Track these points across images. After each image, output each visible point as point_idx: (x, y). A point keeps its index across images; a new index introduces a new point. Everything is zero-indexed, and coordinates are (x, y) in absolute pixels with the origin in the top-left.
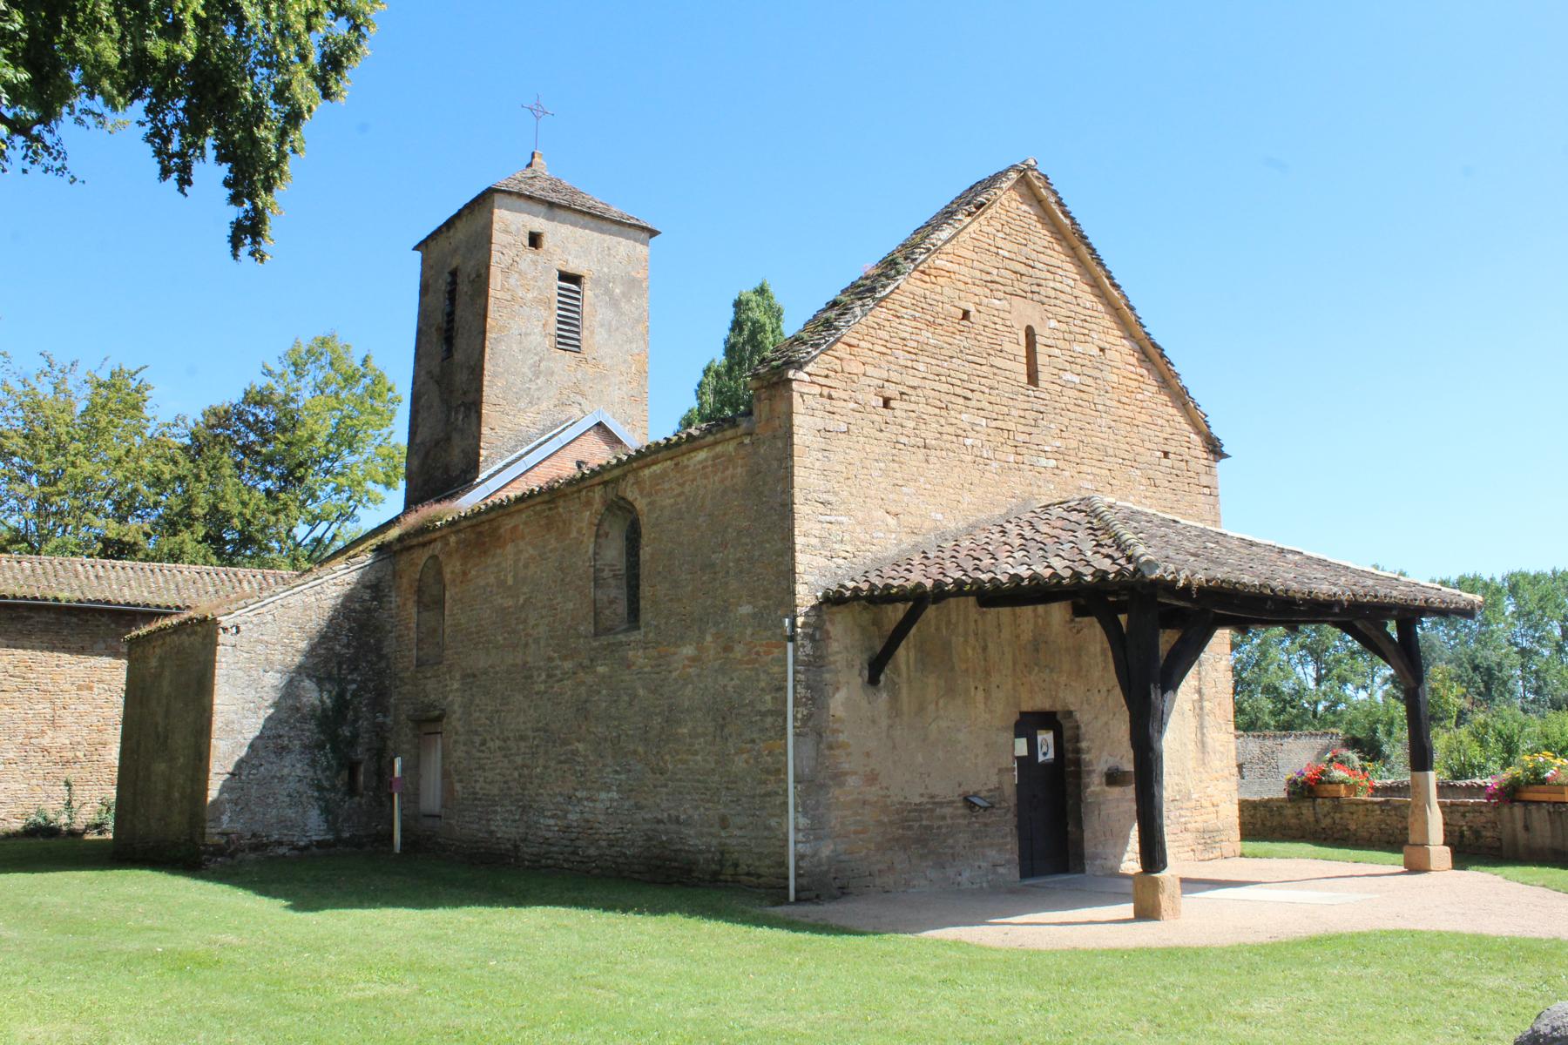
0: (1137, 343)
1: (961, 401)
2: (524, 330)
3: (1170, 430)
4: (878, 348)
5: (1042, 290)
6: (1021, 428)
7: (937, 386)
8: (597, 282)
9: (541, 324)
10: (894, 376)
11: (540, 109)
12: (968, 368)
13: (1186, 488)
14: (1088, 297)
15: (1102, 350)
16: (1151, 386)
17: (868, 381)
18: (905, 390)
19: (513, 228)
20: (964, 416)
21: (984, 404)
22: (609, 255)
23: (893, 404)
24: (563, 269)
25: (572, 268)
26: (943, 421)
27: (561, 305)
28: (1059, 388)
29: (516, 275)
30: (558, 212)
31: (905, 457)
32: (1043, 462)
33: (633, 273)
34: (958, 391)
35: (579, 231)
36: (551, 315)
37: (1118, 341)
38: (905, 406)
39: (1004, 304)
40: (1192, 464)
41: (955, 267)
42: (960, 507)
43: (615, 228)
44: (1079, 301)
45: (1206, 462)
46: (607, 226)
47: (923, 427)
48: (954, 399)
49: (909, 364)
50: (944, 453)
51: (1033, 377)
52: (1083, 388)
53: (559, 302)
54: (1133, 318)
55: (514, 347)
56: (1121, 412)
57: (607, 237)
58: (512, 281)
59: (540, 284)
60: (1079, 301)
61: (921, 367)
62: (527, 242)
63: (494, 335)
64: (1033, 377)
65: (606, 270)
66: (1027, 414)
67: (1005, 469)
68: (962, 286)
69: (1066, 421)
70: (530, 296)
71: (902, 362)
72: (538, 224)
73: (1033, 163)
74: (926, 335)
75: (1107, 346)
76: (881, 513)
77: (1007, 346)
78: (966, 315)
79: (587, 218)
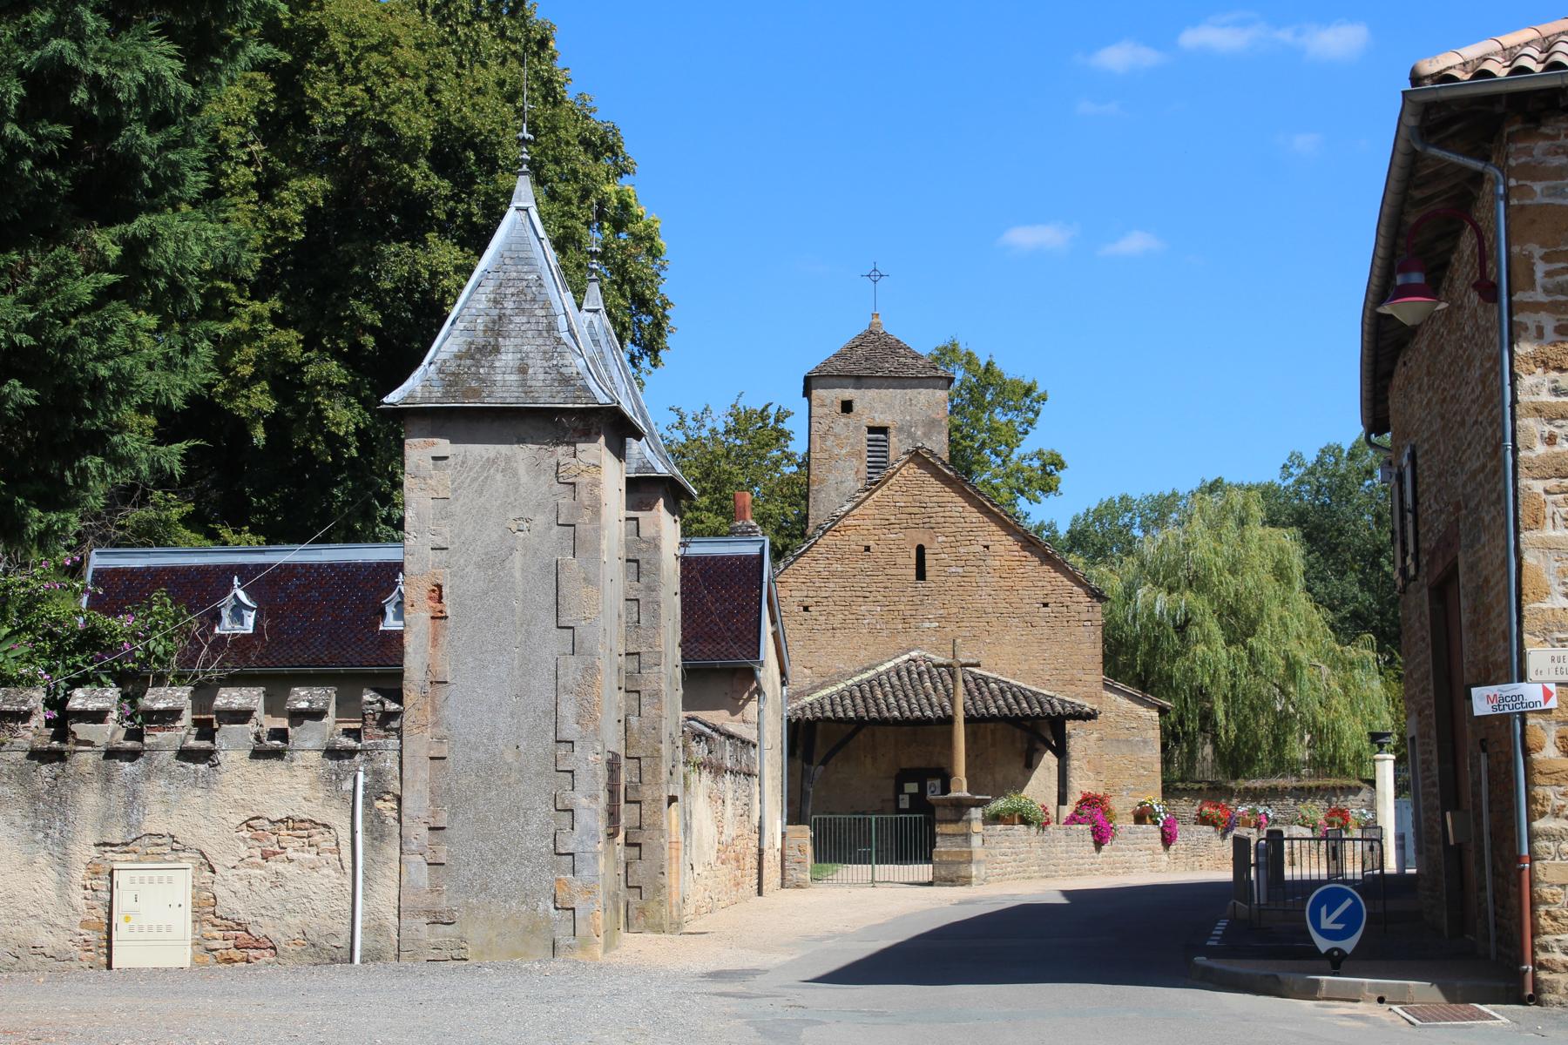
0: (1022, 535)
1: (861, 599)
2: (840, 479)
3: (1050, 588)
4: (800, 580)
5: (932, 520)
6: (908, 607)
7: (842, 594)
8: (900, 430)
9: (853, 472)
10: (811, 594)
11: (877, 273)
12: (868, 580)
13: (1065, 624)
14: (974, 515)
15: (987, 547)
16: (1035, 561)
17: (792, 599)
18: (819, 599)
19: (828, 401)
20: (862, 608)
21: (880, 598)
22: (911, 405)
23: (810, 609)
24: (871, 425)
25: (878, 423)
26: (846, 613)
27: (870, 454)
28: (943, 578)
29: (832, 438)
30: (864, 381)
31: (818, 636)
32: (927, 625)
33: (933, 416)
34: (858, 594)
35: (883, 391)
36: (861, 464)
37: (1004, 538)
38: (818, 608)
39: (901, 536)
40: (1074, 607)
41: (861, 522)
42: (858, 659)
43: (916, 381)
44: (966, 520)
45: (1089, 604)
46: (907, 383)
47: (832, 618)
48: (855, 599)
49: (823, 585)
50: (847, 631)
51: (921, 574)
52: (965, 574)
53: (869, 451)
54: (1012, 522)
55: (833, 494)
56: (1002, 584)
57: (909, 391)
58: (828, 443)
59: (852, 440)
60: (966, 520)
61: (831, 585)
62: (839, 410)
63: (816, 488)
64: (921, 574)
65: (908, 418)
66: (914, 599)
67: (894, 633)
68: (866, 532)
69: (949, 597)
70: (844, 452)
71: (817, 585)
72: (848, 394)
73: (920, 445)
74: (837, 567)
75: (989, 543)
76: (800, 668)
77: (899, 561)
78: (868, 549)
79: (890, 380)
